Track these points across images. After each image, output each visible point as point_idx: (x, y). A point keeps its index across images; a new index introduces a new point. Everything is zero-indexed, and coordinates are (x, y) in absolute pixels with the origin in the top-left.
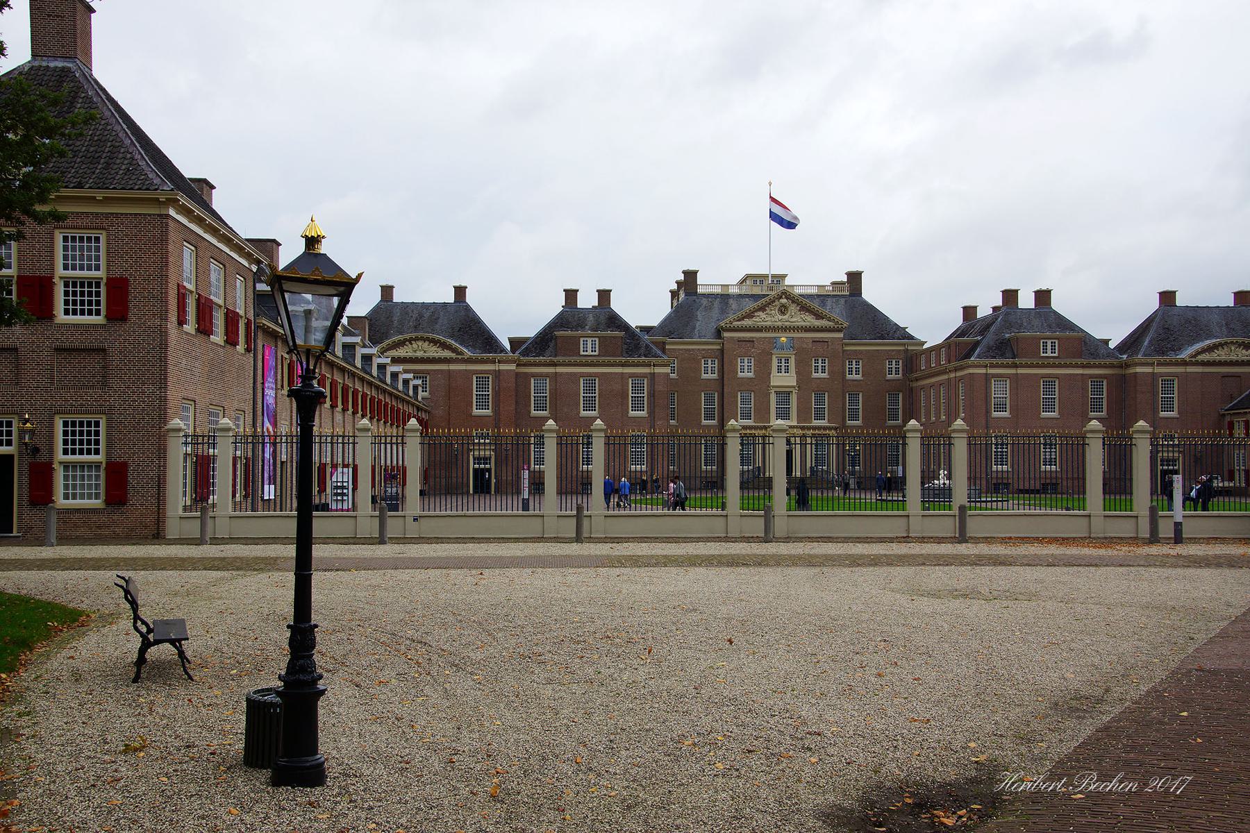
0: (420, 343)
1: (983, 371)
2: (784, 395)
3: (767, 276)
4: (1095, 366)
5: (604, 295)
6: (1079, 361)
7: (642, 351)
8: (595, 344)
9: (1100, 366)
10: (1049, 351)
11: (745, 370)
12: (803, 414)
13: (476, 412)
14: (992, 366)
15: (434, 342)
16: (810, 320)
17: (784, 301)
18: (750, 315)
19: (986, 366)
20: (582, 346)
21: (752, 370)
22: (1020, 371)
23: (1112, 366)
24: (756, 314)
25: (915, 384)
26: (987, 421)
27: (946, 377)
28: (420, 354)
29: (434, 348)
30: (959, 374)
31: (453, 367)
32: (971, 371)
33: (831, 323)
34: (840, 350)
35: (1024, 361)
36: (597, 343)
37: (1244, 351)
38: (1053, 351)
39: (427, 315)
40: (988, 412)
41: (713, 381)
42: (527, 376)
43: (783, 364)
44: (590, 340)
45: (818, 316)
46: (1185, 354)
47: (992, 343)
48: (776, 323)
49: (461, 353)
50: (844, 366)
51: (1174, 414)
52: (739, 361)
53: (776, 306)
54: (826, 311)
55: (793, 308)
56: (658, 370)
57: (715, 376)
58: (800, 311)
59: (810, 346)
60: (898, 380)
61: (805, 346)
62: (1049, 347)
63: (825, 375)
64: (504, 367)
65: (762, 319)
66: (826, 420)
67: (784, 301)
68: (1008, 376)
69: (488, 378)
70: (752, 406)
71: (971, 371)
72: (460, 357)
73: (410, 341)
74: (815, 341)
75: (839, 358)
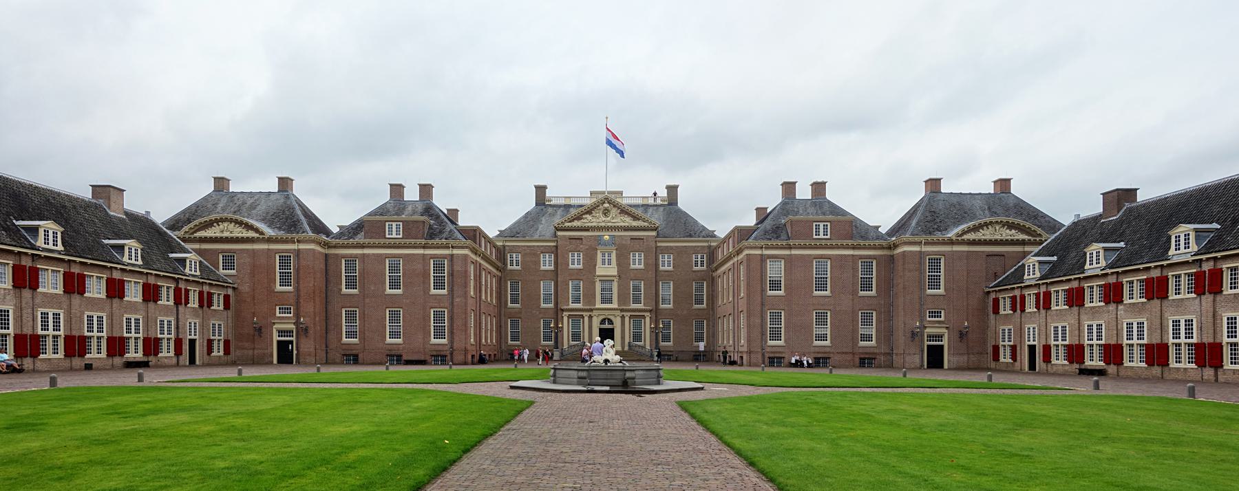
1: (758, 252)
2: (606, 280)
3: (604, 193)
7: (444, 235)
8: (399, 228)
11: (575, 262)
14: (768, 248)
15: (240, 223)
16: (628, 221)
17: (606, 205)
18: (579, 218)
19: (762, 248)
20: (387, 229)
21: (581, 263)
22: (794, 252)
24: (584, 216)
25: (714, 274)
26: (762, 298)
27: (731, 262)
30: (741, 257)
33: (646, 224)
34: (654, 246)
35: (797, 242)
36: (401, 227)
39: (250, 201)
40: (763, 290)
41: (550, 272)
43: (607, 258)
45: (635, 218)
47: (769, 227)
48: (600, 224)
50: (657, 259)
52: (570, 255)
53: (600, 209)
54: (647, 216)
55: (614, 211)
56: (456, 252)
57: (552, 268)
58: (620, 213)
60: (703, 271)
61: (624, 242)
63: (642, 266)
65: (589, 221)
66: (642, 304)
67: (606, 205)
69: (290, 257)
70: (581, 292)
71: (746, 252)
75: (654, 254)
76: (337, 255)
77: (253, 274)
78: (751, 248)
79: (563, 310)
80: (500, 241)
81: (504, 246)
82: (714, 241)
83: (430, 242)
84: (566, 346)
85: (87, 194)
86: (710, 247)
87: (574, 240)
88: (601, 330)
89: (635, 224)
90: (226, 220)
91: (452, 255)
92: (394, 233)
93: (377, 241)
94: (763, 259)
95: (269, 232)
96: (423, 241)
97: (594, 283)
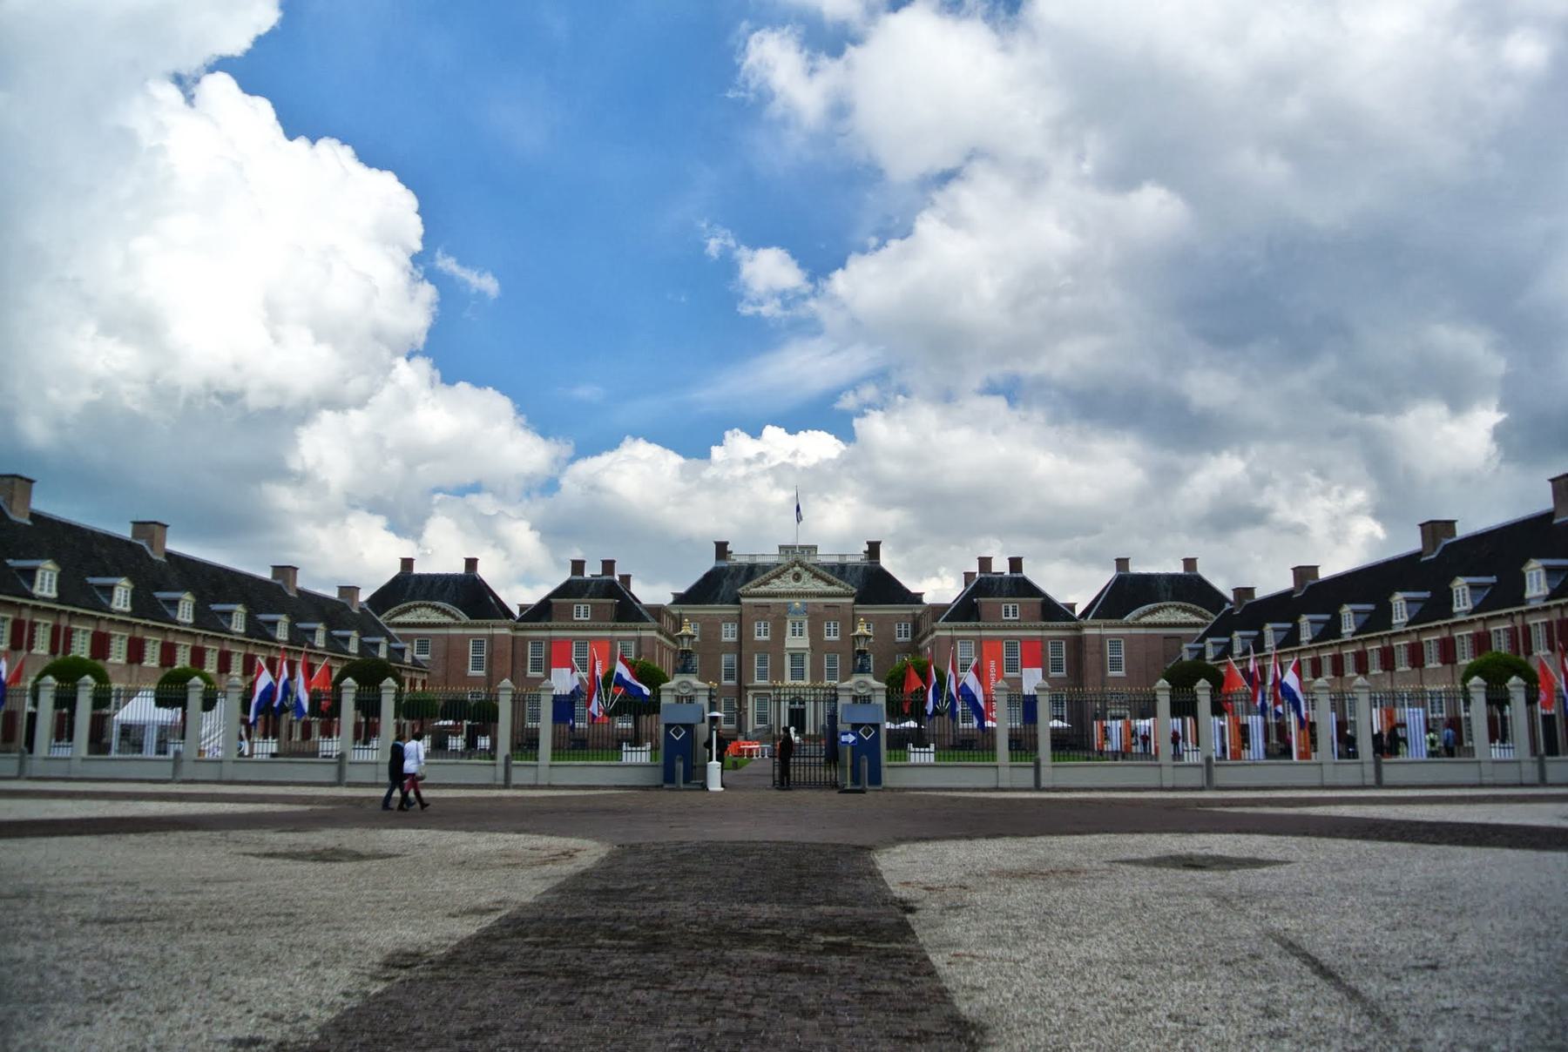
0: (423, 610)
1: (948, 633)
2: (797, 658)
3: (795, 547)
4: (1052, 629)
5: (608, 566)
6: (1039, 624)
9: (1058, 629)
10: (1011, 614)
11: (761, 632)
12: (817, 675)
13: (471, 672)
14: (957, 629)
17: (797, 569)
18: (766, 583)
19: (951, 629)
23: (1069, 628)
24: (772, 581)
28: (423, 620)
29: (436, 614)
31: (452, 631)
32: (938, 633)
33: (842, 589)
34: (850, 613)
37: (1183, 615)
38: (1014, 614)
42: (525, 640)
43: (797, 627)
44: (582, 607)
45: (830, 583)
46: (1129, 618)
49: (458, 619)
51: (1122, 673)
55: (806, 576)
56: (644, 634)
59: (822, 610)
61: (817, 611)
62: (1011, 611)
64: (497, 631)
67: (797, 569)
68: (972, 638)
72: (457, 622)
73: (415, 607)
74: (827, 606)
76: (524, 638)
77: (447, 658)
78: (941, 629)
79: (747, 688)
80: (675, 609)
81: (681, 614)
82: (919, 608)
83: (618, 624)
84: (750, 730)
85: (333, 594)
86: (914, 615)
87: (760, 609)
88: (791, 711)
89: (830, 589)
90: (424, 606)
91: (640, 638)
92: (582, 615)
93: (565, 624)
94: (953, 640)
95: (465, 619)
96: (612, 624)
97: (783, 656)
